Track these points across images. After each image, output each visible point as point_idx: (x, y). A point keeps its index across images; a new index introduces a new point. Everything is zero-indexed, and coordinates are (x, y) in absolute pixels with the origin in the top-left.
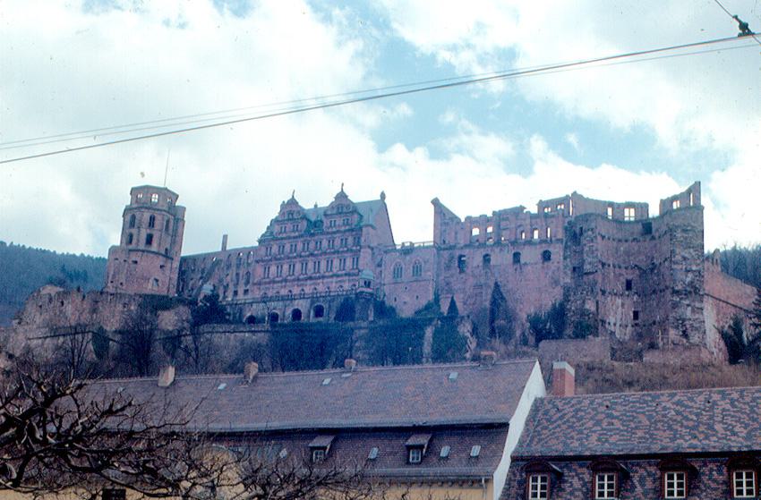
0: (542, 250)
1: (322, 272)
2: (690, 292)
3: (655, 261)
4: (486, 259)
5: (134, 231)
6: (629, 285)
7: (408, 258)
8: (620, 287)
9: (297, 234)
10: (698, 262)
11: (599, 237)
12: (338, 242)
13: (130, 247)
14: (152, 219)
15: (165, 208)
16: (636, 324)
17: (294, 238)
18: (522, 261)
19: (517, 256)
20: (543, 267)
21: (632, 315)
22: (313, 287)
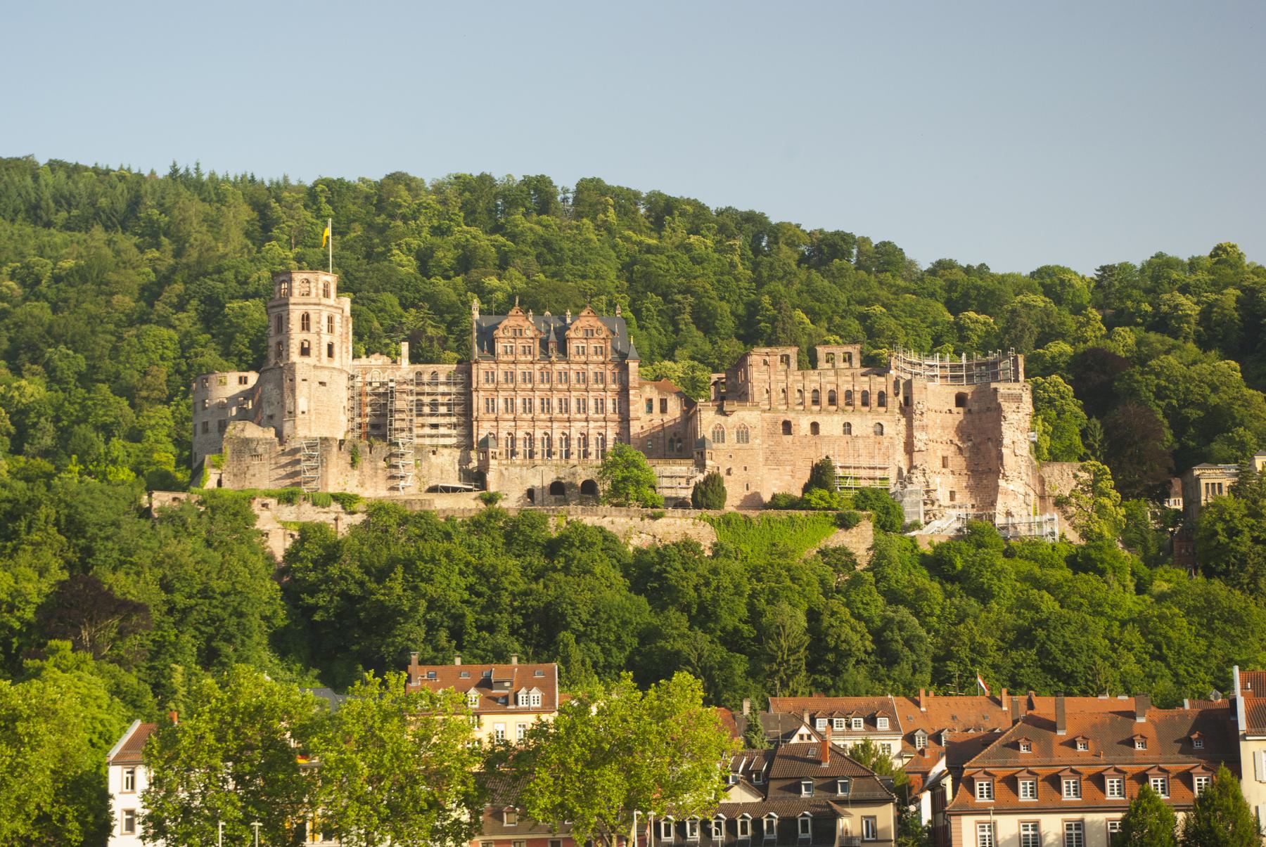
4: (815, 427)
7: (730, 419)
14: (330, 320)
19: (848, 427)
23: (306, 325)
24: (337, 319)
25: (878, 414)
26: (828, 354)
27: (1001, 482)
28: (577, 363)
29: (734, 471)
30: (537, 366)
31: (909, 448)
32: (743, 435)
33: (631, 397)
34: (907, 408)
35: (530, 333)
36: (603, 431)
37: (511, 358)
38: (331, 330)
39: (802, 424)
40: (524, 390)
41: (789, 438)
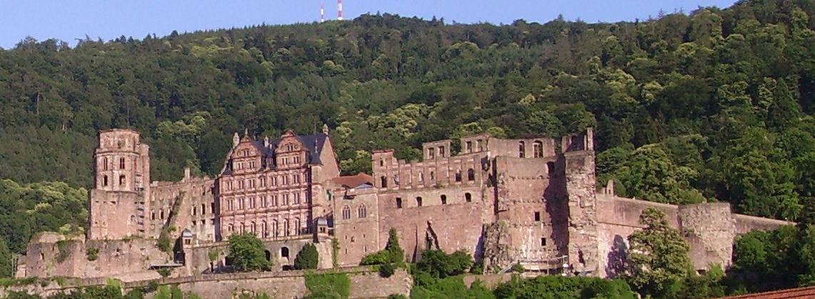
0: (464, 192)
1: (280, 205)
2: (585, 224)
3: (557, 196)
4: (419, 199)
5: (108, 173)
6: (537, 217)
7: (353, 201)
8: (531, 218)
9: (253, 170)
10: (590, 199)
11: (510, 179)
12: (291, 177)
13: (106, 189)
14: (122, 160)
15: (132, 149)
16: (545, 249)
17: (250, 173)
18: (448, 203)
19: (444, 198)
20: (465, 208)
21: (541, 241)
22: (272, 218)
23: (106, 168)
24: (127, 159)
25: (466, 185)
26: (468, 143)
27: (571, 229)
28: (282, 170)
29: (355, 239)
30: (258, 175)
31: (496, 211)
32: (363, 213)
33: (313, 190)
34: (493, 181)
35: (253, 153)
36: (298, 216)
37: (242, 172)
38: (122, 166)
39: (410, 200)
40: (249, 193)
41: (401, 209)
